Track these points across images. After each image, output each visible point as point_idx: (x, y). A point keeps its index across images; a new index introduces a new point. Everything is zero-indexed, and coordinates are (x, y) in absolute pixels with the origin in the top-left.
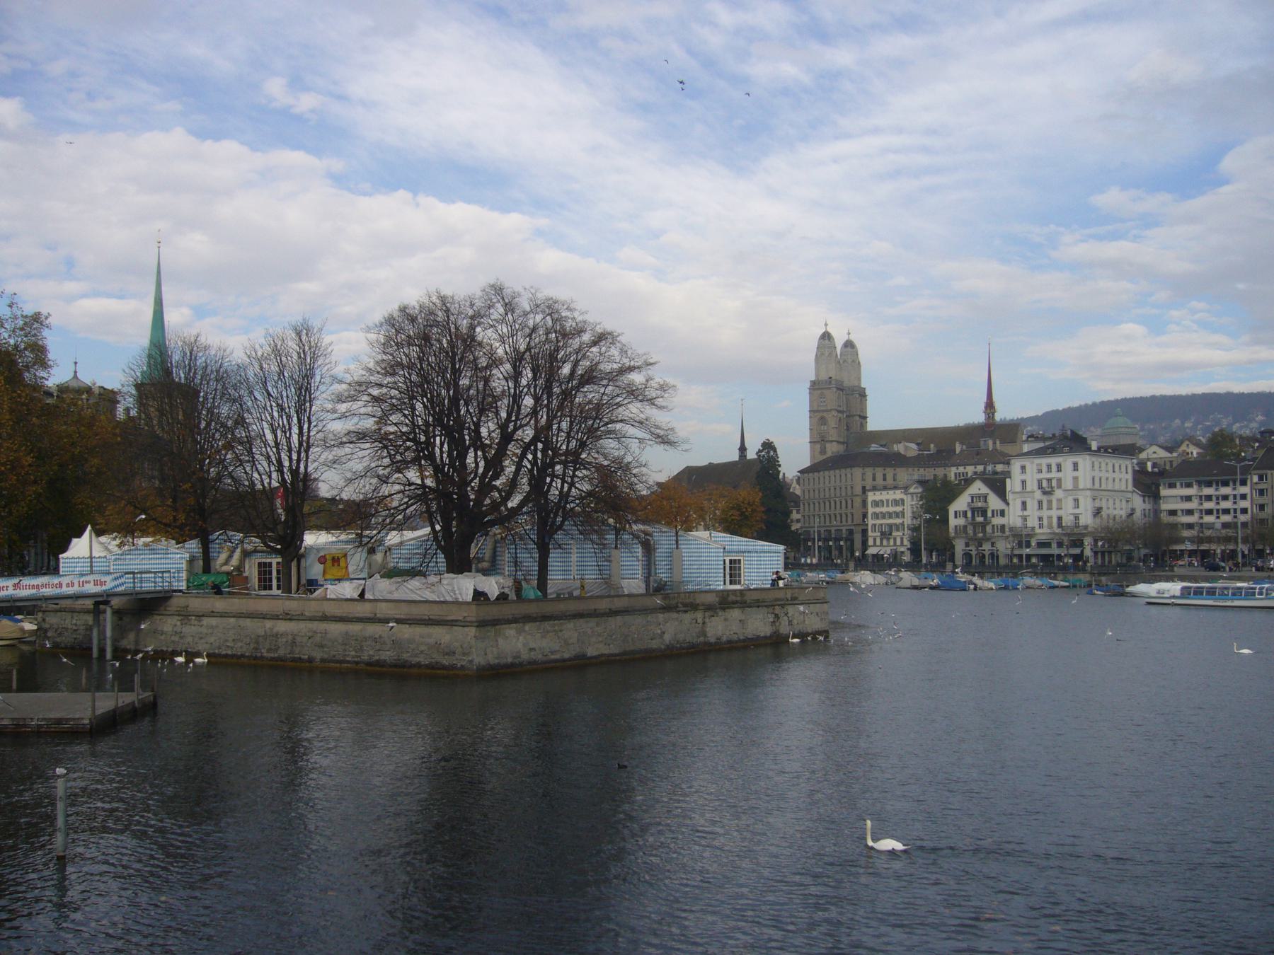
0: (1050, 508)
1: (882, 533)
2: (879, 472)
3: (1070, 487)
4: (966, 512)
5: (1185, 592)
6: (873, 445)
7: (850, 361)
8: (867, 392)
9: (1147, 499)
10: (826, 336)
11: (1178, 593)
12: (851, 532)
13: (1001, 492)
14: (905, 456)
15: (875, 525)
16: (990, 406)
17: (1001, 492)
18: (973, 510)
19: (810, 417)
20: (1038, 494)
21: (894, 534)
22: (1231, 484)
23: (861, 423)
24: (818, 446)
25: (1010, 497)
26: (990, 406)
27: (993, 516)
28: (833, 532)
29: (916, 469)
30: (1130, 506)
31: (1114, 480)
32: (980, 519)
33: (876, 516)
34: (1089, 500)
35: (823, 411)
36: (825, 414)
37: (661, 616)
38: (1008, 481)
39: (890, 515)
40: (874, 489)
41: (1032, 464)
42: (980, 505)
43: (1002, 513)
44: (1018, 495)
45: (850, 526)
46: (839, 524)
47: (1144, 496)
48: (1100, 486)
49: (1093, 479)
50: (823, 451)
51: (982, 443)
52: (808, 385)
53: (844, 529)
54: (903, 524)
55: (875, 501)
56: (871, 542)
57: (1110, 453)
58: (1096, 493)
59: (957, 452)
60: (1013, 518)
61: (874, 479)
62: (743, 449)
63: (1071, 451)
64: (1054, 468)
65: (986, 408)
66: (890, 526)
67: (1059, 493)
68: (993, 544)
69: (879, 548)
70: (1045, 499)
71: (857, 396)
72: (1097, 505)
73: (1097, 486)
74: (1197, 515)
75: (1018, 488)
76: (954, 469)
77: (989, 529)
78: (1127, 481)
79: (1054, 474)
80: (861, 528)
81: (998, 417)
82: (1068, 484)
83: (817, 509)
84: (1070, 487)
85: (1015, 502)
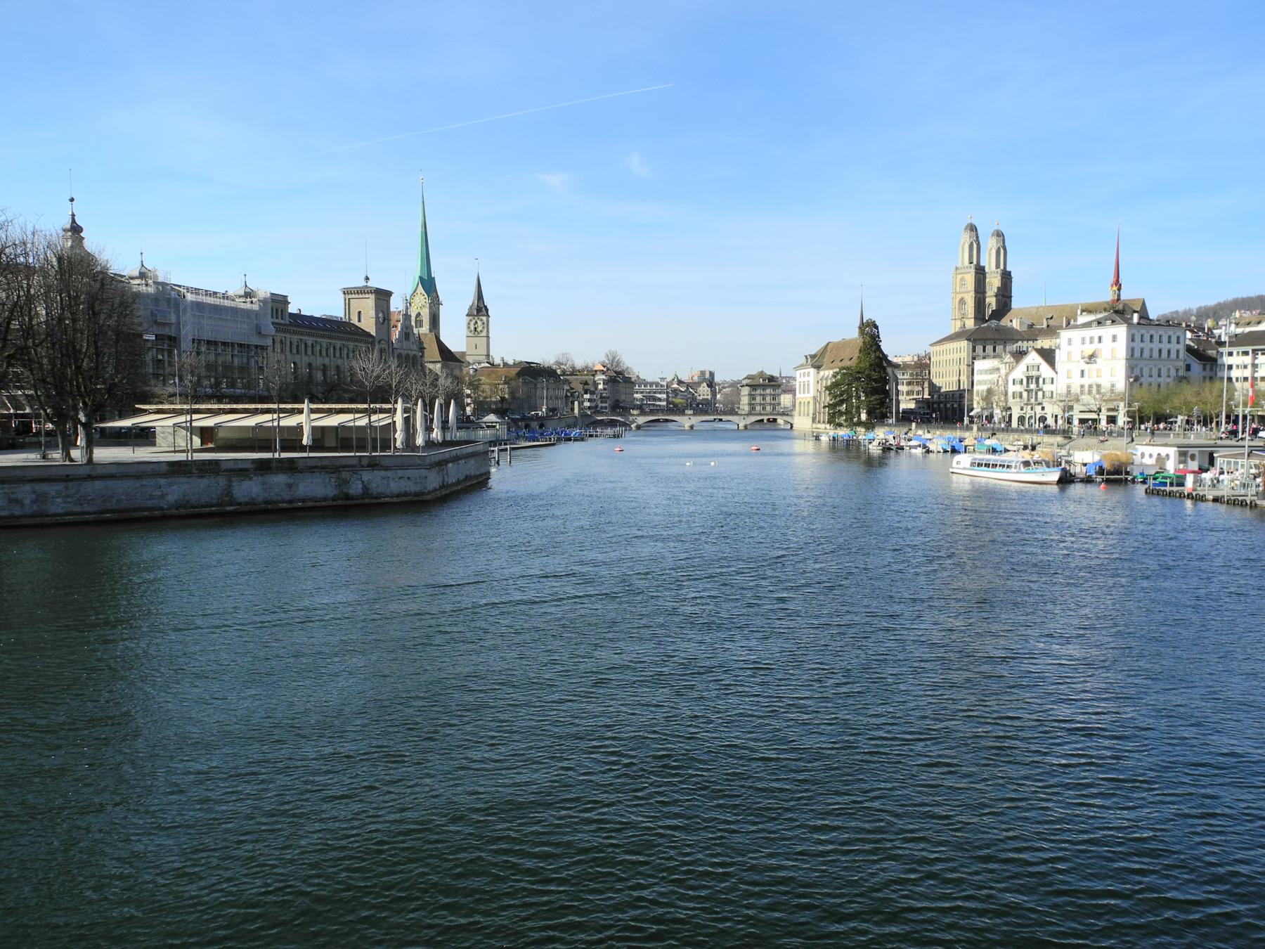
5: (973, 464)
10: (972, 228)
16: (1117, 283)
18: (1028, 378)
23: (1005, 303)
26: (1117, 283)
29: (1025, 342)
33: (980, 383)
37: (162, 481)
38: (1057, 351)
41: (1075, 335)
42: (1034, 373)
61: (984, 351)
68: (1043, 408)
72: (1137, 372)
73: (1137, 354)
78: (1178, 351)
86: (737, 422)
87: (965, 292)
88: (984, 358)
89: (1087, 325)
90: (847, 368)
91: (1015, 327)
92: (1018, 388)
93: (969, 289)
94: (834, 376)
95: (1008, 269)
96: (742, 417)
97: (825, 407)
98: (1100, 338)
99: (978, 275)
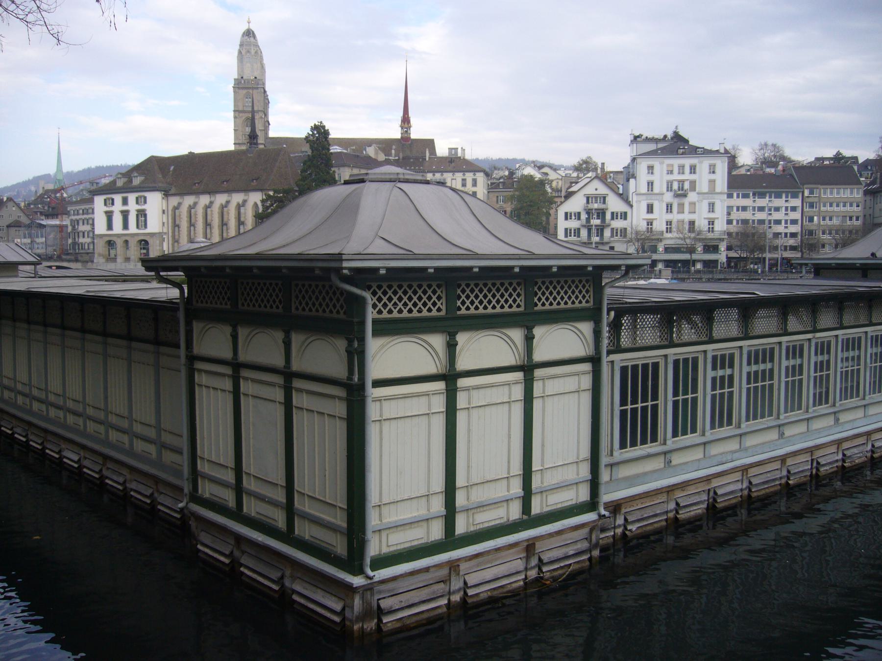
4: (579, 213)
16: (406, 120)
18: (589, 212)
20: (668, 197)
26: (406, 120)
27: (612, 218)
43: (624, 216)
44: (644, 197)
59: (427, 159)
67: (692, 196)
75: (644, 189)
77: (607, 233)
79: (687, 176)
82: (703, 187)
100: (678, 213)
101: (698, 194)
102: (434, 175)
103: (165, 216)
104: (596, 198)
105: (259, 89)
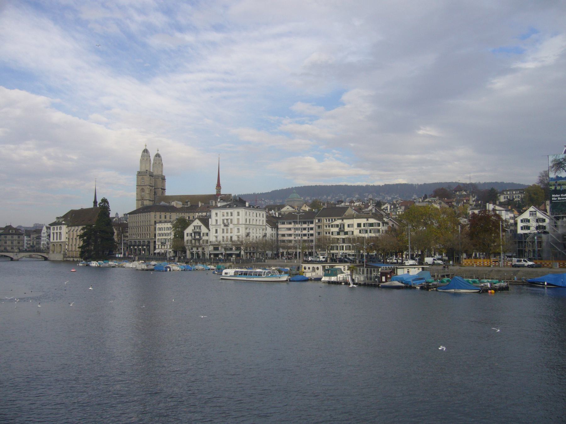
0: (227, 233)
1: (162, 243)
2: (163, 214)
3: (236, 223)
4: (192, 233)
5: (236, 274)
6: (162, 202)
7: (158, 163)
8: (166, 178)
9: (273, 229)
10: (146, 151)
11: (233, 274)
12: (149, 242)
13: (207, 225)
14: (176, 207)
15: (159, 239)
16: (219, 186)
17: (207, 225)
18: (195, 233)
19: (137, 188)
20: (222, 226)
21: (167, 243)
22: (307, 223)
24: (140, 202)
25: (211, 227)
26: (219, 186)
28: (142, 242)
29: (180, 214)
30: (264, 232)
31: (256, 220)
32: (197, 237)
33: (160, 235)
34: (244, 229)
35: (144, 186)
36: (143, 187)
38: (210, 219)
39: (166, 235)
40: (160, 222)
41: (220, 212)
42: (198, 230)
44: (214, 226)
45: (148, 239)
46: (144, 238)
47: (272, 228)
48: (250, 223)
49: (246, 220)
50: (142, 204)
51: (210, 202)
52: (136, 173)
53: (146, 241)
54: (170, 239)
55: (168, 227)
56: (157, 247)
57: (255, 208)
58: (247, 226)
59: (199, 206)
60: (212, 238)
61: (160, 218)
62: (95, 202)
63: (237, 206)
64: (229, 214)
65: (217, 187)
66: (165, 239)
67: (231, 226)
69: (160, 250)
70: (225, 228)
71: (161, 179)
72: (248, 231)
73: (248, 223)
74: (293, 236)
75: (214, 223)
76: (197, 214)
77: (201, 242)
79: (229, 217)
80: (153, 240)
81: (222, 192)
82: (235, 222)
83: (133, 231)
84: (236, 223)
85: (213, 230)
86: (12, 256)
87: (144, 186)
88: (165, 222)
89: (224, 207)
90: (91, 226)
91: (175, 206)
92: (190, 238)
93: (146, 184)
94: (83, 229)
95: (164, 175)
96: (15, 253)
97: (79, 248)
98: (231, 213)
99: (150, 177)
100: (226, 233)
101: (233, 225)
102: (199, 214)
103: (67, 235)
104: (198, 227)
105: (147, 175)
